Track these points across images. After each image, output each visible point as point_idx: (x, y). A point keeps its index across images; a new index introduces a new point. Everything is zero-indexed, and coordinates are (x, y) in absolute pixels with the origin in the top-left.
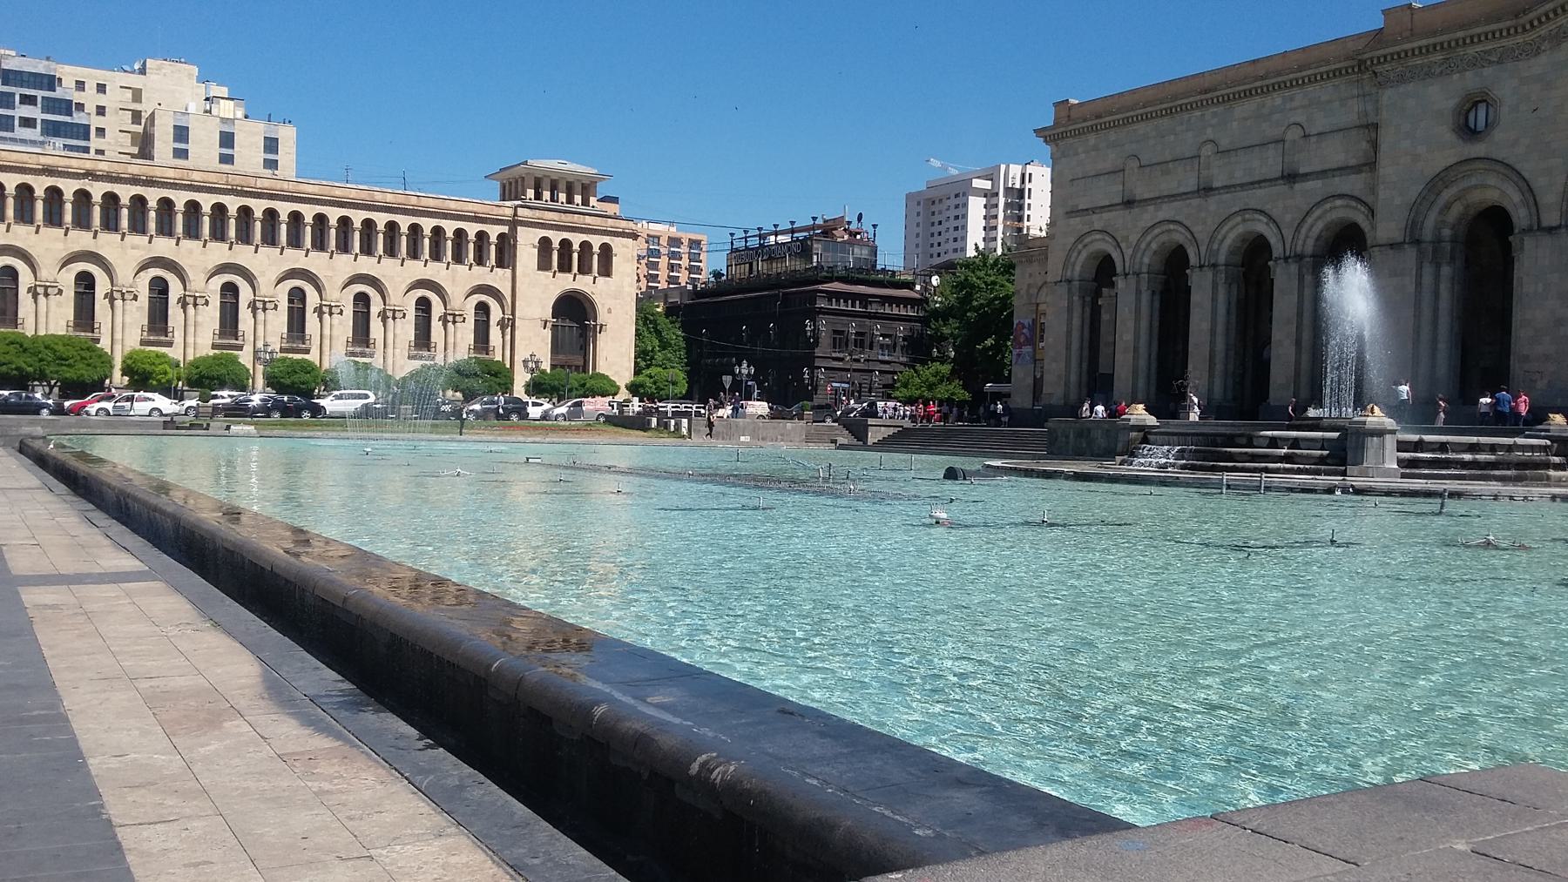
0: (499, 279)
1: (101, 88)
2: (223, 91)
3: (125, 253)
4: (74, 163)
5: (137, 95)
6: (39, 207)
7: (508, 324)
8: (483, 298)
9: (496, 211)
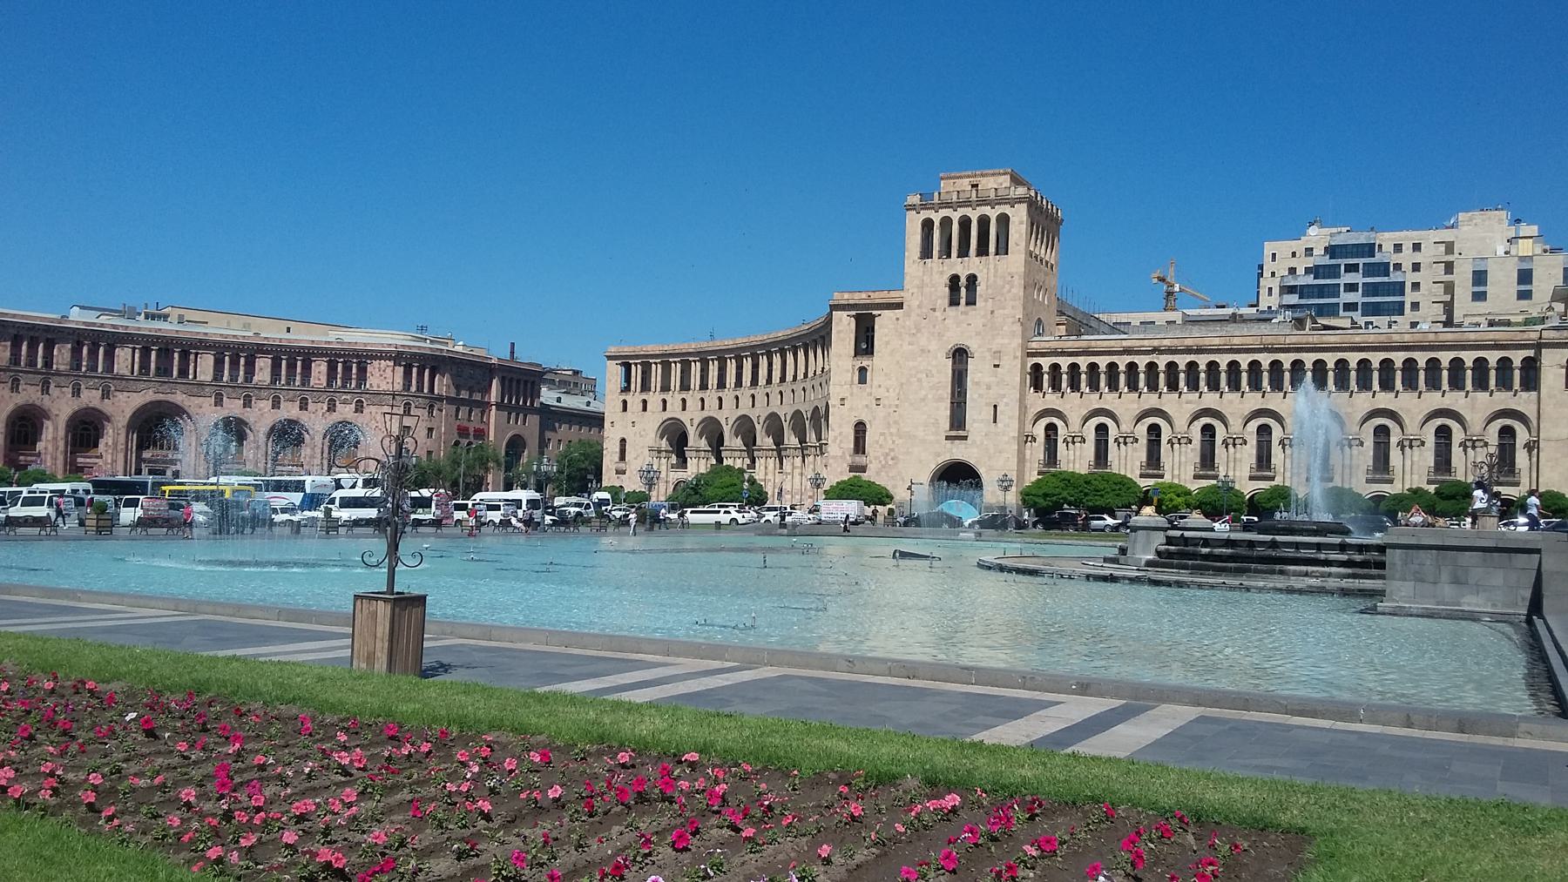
0: (1523, 401)
1: (1417, 247)
2: (1533, 230)
3: (1180, 406)
4: (1146, 343)
5: (1450, 248)
6: (1122, 378)
7: (1531, 447)
8: (1508, 422)
9: (1519, 336)
